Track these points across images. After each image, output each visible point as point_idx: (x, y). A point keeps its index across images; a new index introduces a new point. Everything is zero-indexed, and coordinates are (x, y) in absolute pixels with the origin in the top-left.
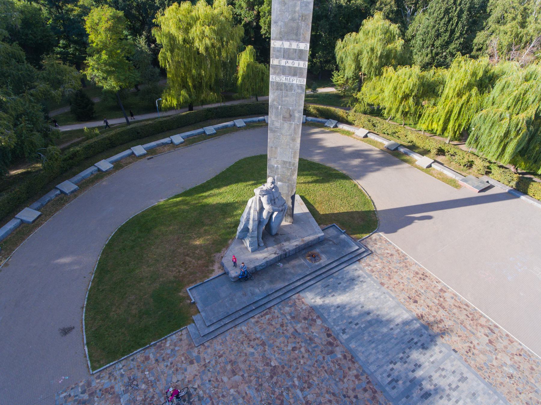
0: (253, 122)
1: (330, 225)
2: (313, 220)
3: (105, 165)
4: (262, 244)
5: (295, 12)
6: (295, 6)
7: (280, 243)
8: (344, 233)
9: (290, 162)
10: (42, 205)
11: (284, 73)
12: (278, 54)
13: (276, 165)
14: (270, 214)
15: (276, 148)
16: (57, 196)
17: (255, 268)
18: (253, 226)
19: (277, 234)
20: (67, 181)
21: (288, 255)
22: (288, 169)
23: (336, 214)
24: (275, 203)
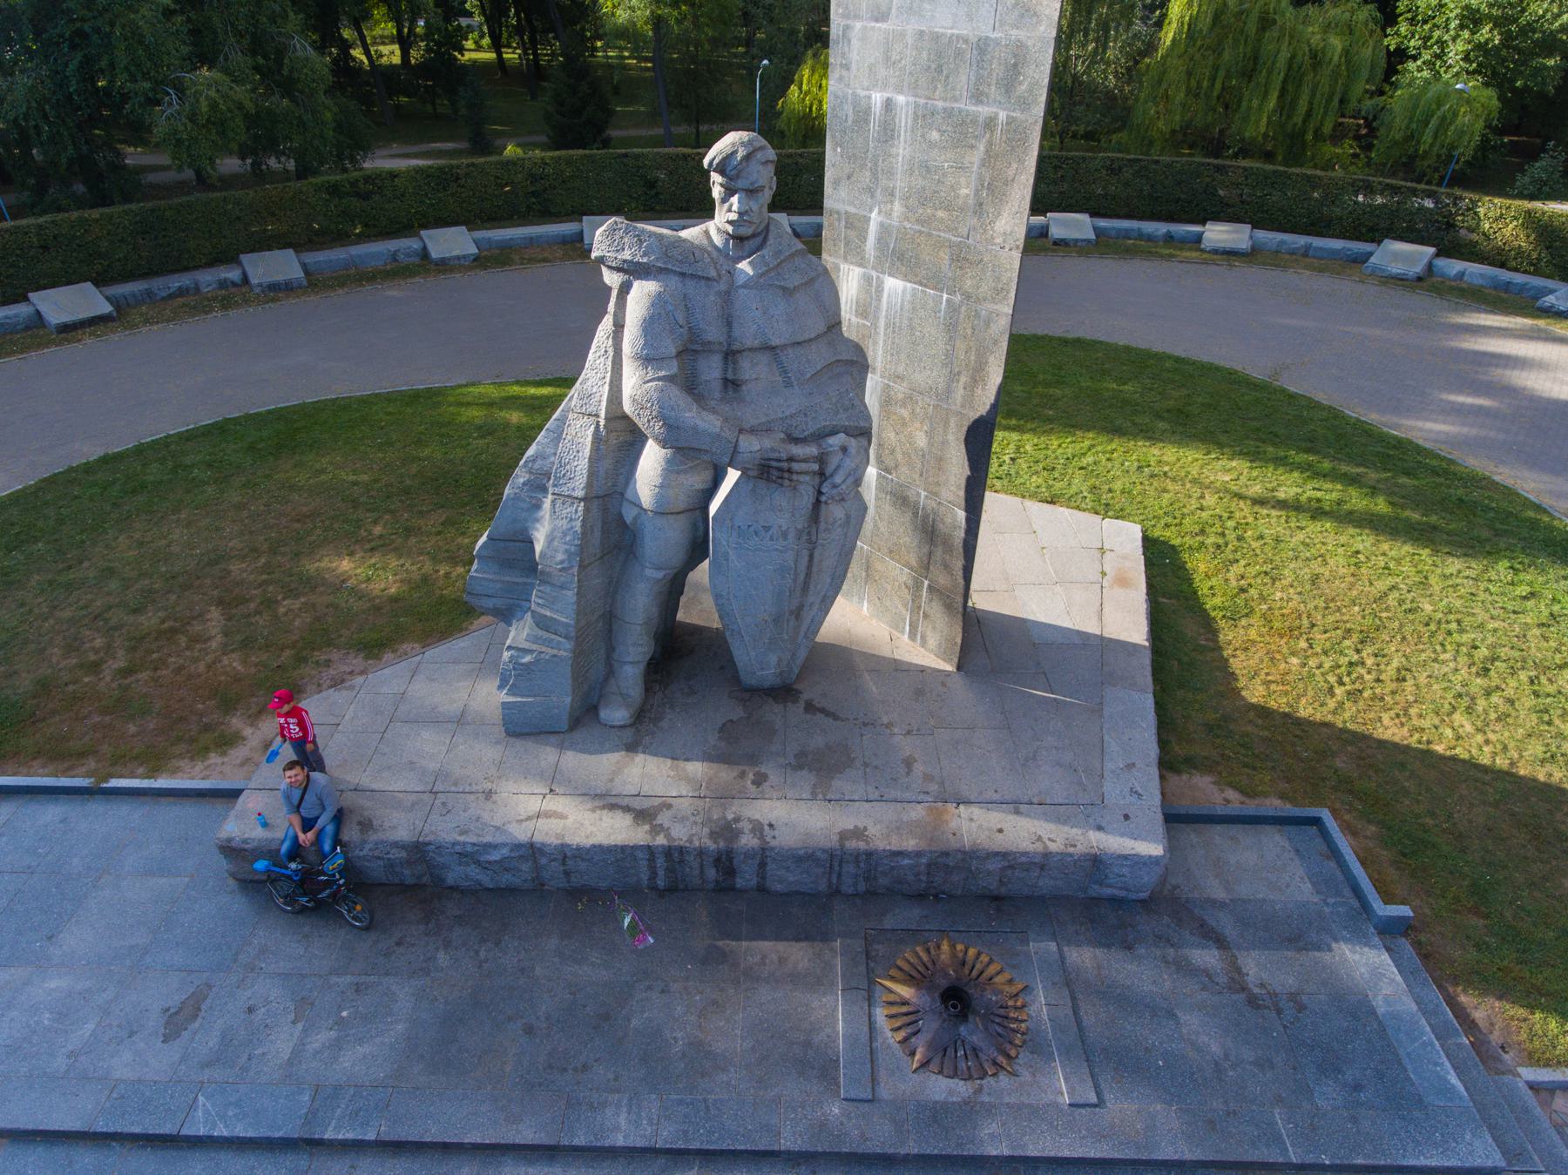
0: (1140, 236)
1: (1274, 805)
2: (1135, 709)
3: (451, 242)
4: (616, 714)
7: (752, 759)
8: (1390, 931)
10: (149, 293)
13: (877, 98)
14: (698, 481)
16: (223, 284)
17: (419, 851)
18: (550, 539)
19: (783, 692)
20: (291, 251)
21: (746, 878)
22: (962, 130)
23: (1382, 743)
24: (732, 385)
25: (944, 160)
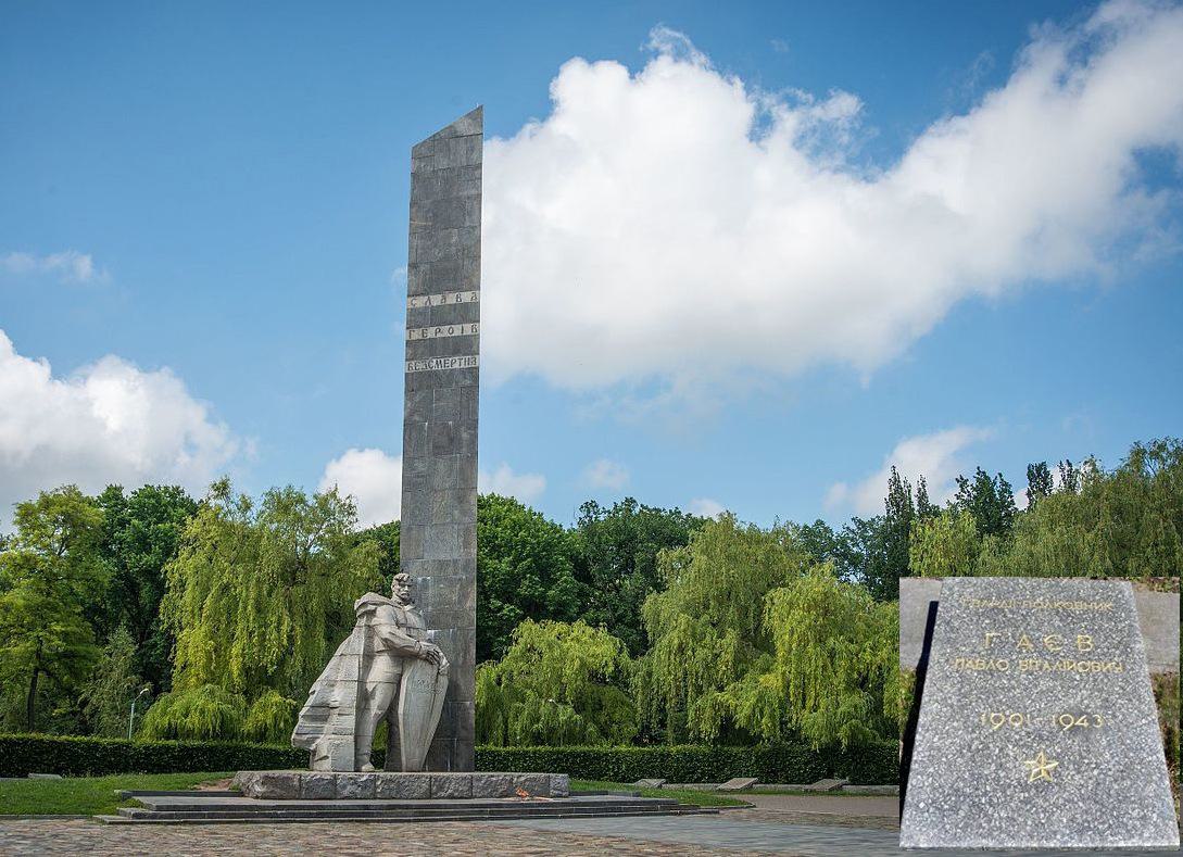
5: (450, 245)
6: (449, 236)
9: (455, 562)
11: (433, 354)
12: (420, 319)
15: (421, 526)
22: (451, 583)
25: (447, 591)
